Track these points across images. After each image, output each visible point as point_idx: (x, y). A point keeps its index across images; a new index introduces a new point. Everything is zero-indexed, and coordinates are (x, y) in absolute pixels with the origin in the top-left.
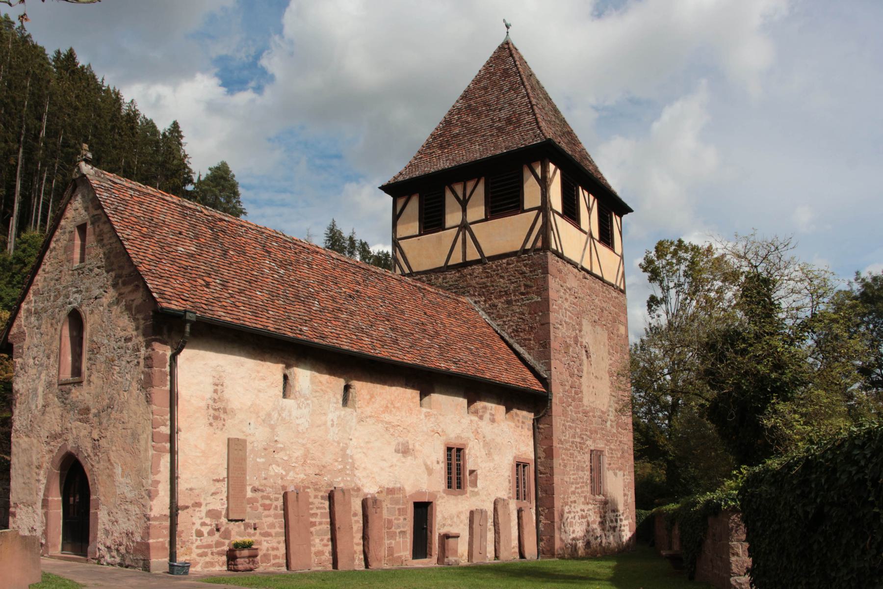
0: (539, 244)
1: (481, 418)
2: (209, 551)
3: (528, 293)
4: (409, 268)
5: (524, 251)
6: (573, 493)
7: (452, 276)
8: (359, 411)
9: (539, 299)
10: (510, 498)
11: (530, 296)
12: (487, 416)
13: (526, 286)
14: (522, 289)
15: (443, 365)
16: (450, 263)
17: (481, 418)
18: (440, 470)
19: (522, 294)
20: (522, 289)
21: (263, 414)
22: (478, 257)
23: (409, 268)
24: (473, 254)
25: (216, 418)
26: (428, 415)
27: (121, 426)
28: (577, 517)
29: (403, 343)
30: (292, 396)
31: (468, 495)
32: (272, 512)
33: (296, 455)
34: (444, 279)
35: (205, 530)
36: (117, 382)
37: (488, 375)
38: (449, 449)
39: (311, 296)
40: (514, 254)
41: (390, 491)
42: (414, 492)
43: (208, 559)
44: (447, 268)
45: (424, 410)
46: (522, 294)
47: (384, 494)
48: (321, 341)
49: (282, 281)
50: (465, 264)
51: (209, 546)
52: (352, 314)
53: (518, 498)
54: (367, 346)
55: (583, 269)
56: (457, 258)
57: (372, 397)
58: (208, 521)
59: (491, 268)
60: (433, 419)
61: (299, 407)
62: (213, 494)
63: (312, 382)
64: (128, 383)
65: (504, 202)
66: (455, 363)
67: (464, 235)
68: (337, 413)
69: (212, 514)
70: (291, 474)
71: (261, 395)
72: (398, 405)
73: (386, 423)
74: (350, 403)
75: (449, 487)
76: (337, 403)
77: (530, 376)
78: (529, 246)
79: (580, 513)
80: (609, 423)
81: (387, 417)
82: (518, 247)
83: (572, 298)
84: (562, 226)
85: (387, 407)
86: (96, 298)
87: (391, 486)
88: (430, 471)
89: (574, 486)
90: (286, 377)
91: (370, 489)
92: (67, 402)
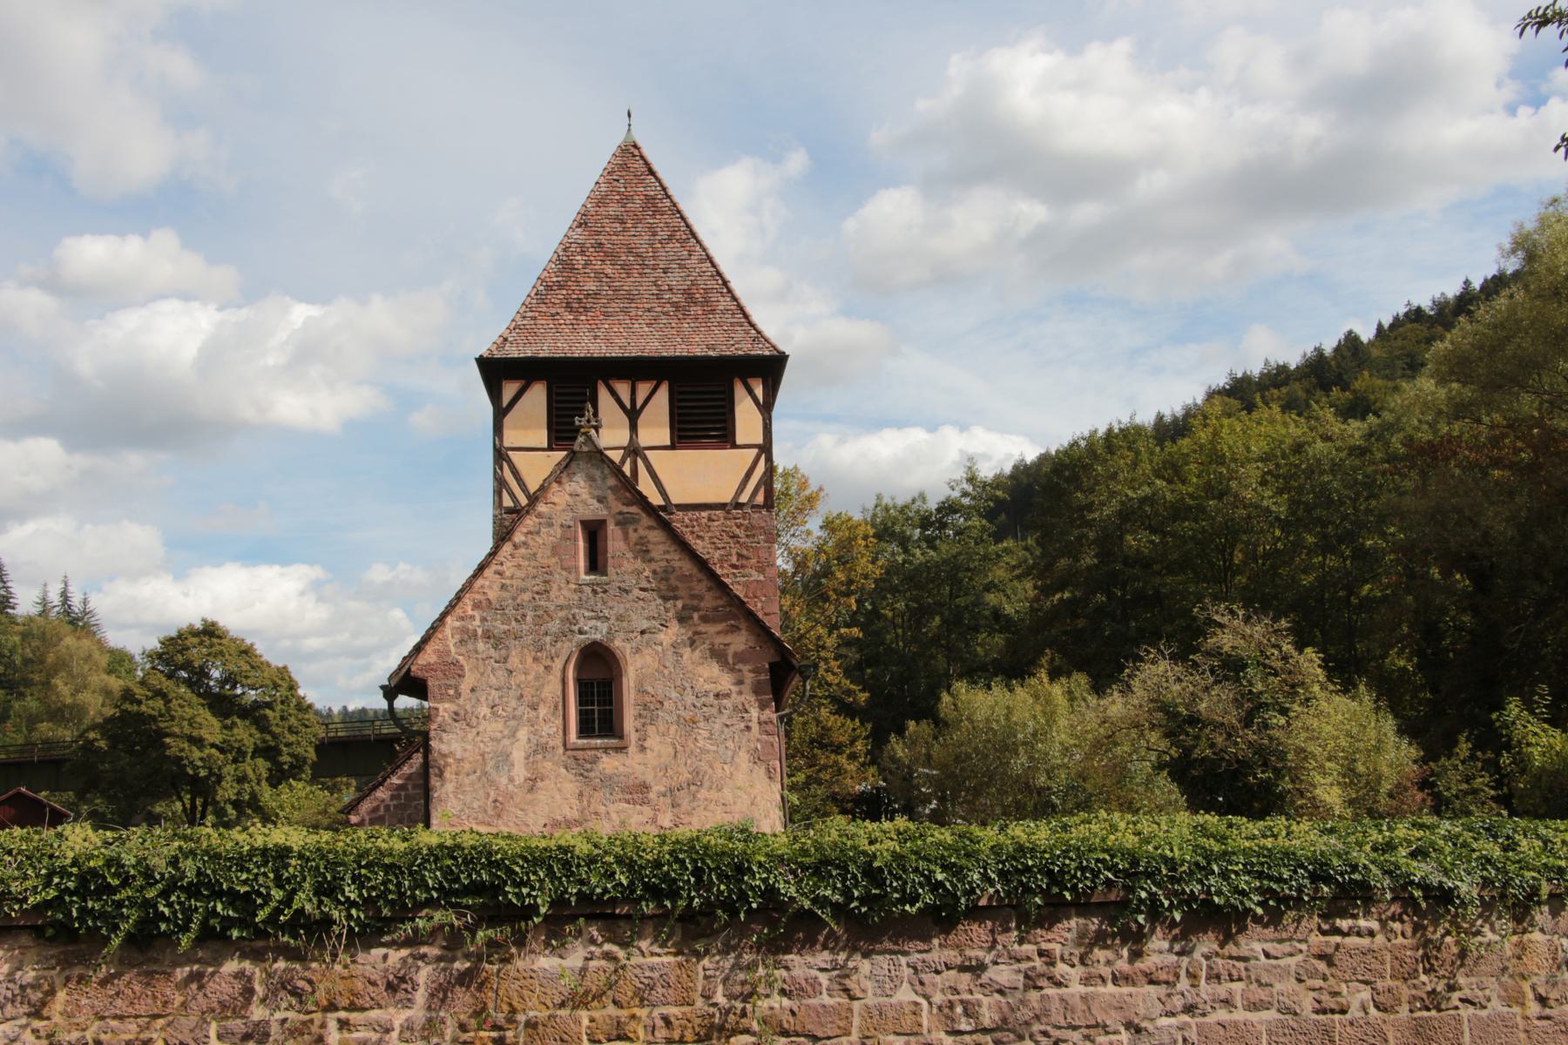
0: (760, 499)
3: (743, 567)
11: (746, 571)
13: (740, 556)
14: (734, 560)
19: (734, 566)
20: (734, 560)
27: (719, 809)
36: (704, 751)
40: (722, 506)
46: (734, 566)
64: (730, 753)
78: (744, 499)
82: (727, 498)
86: (643, 632)
92: (592, 774)
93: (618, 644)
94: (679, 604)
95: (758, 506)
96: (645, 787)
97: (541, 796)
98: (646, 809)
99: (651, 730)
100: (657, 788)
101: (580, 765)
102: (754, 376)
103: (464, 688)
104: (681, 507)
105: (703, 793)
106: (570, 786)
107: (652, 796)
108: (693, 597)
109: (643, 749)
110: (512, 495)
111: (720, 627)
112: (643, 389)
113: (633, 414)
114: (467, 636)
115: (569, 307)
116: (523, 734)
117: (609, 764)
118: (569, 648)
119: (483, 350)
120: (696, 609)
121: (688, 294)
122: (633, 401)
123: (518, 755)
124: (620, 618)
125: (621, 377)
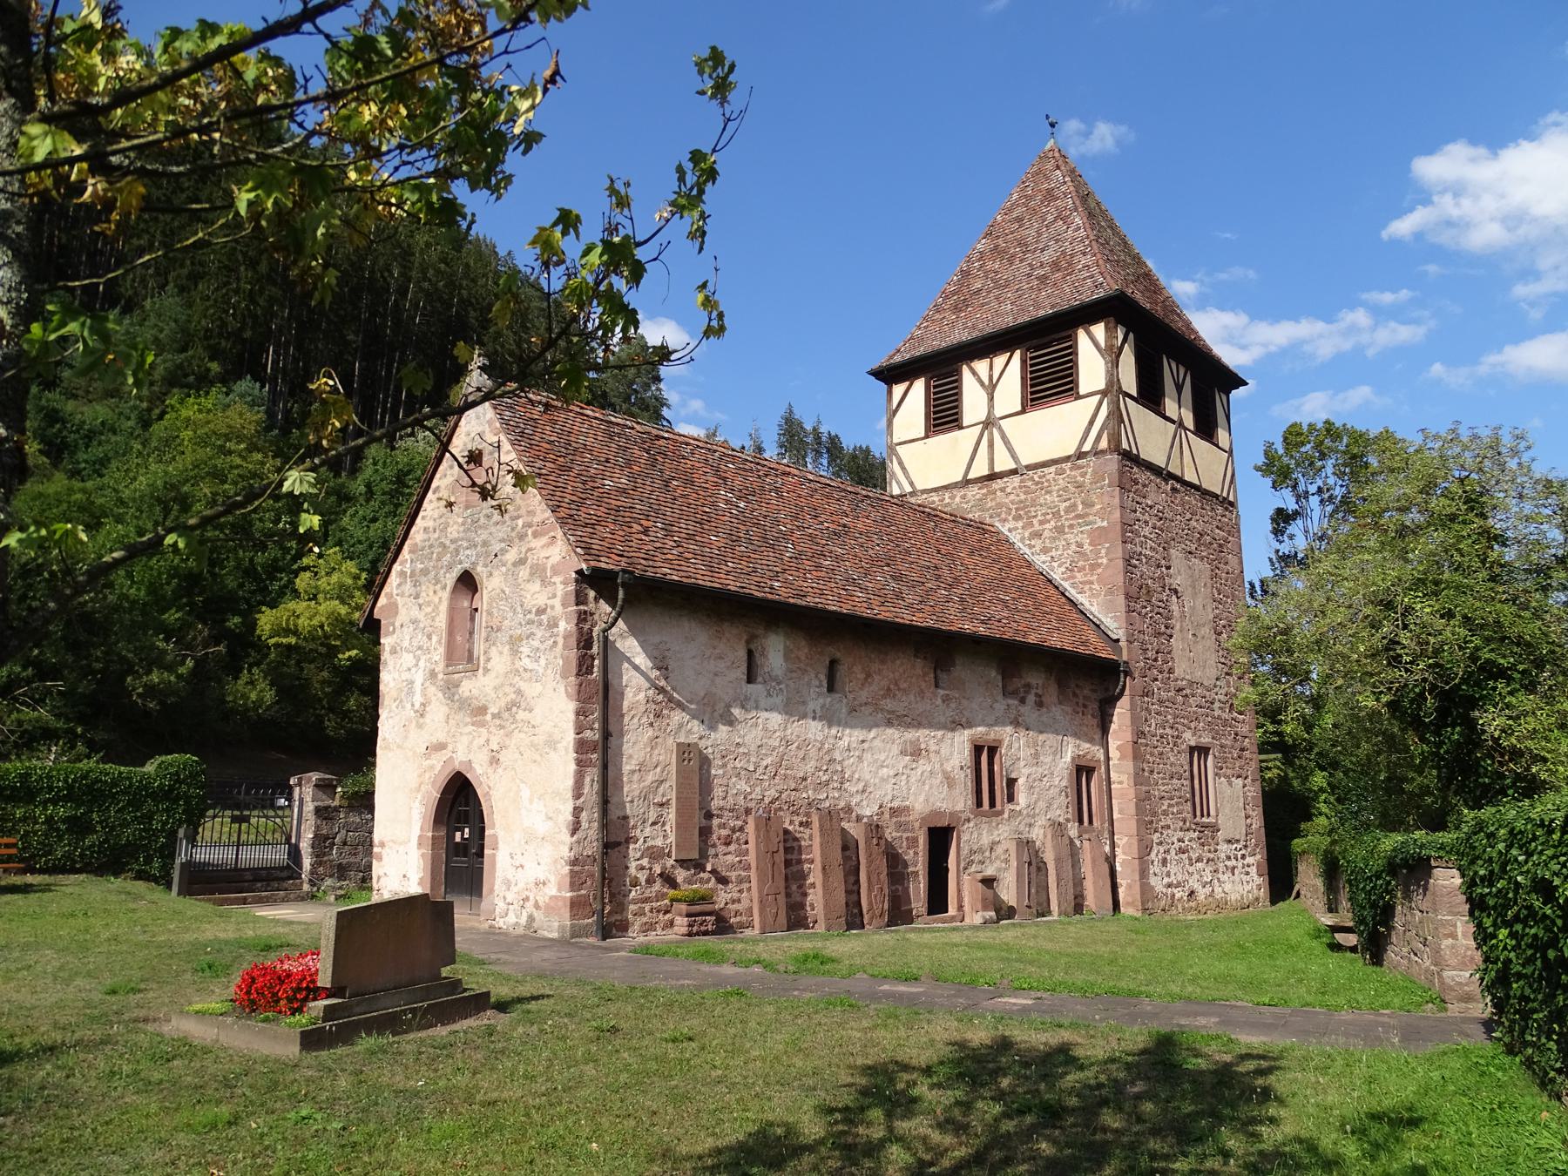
0: (1104, 444)
1: (1023, 701)
2: (647, 908)
3: (1087, 515)
4: (912, 484)
5: (1080, 455)
6: (1165, 813)
7: (974, 492)
8: (851, 696)
9: (1105, 524)
10: (1068, 820)
12: (1031, 698)
15: (968, 627)
16: (971, 476)
17: (1023, 701)
18: (965, 780)
19: (1078, 517)
21: (720, 707)
22: (1013, 466)
23: (912, 484)
24: (1003, 463)
25: (657, 716)
26: (946, 699)
28: (1173, 852)
29: (910, 598)
30: (760, 679)
31: (1006, 815)
32: (732, 848)
33: (764, 763)
34: (963, 497)
35: (642, 876)
37: (1032, 639)
38: (978, 750)
39: (786, 536)
40: (1068, 458)
41: (894, 812)
42: (927, 811)
43: (645, 920)
44: (966, 482)
45: (941, 692)
46: (1078, 517)
47: (887, 816)
48: (799, 602)
49: (742, 517)
50: (992, 477)
51: (646, 900)
52: (838, 558)
53: (1081, 821)
54: (861, 604)
55: (1171, 476)
56: (980, 469)
57: (868, 675)
58: (645, 862)
59: (1032, 479)
60: (953, 705)
61: (769, 695)
62: (654, 824)
63: (787, 657)
65: (1050, 382)
66: (983, 622)
67: (991, 434)
68: (821, 701)
69: (655, 854)
70: (758, 789)
71: (718, 680)
72: (904, 686)
73: (889, 712)
74: (838, 685)
75: (979, 804)
76: (820, 686)
77: (1093, 637)
78: (1087, 447)
79: (1177, 845)
80: (1217, 704)
81: (889, 704)
82: (1071, 451)
83: (1154, 520)
84: (1139, 415)
85: (889, 689)
87: (895, 804)
88: (949, 780)
89: (1166, 803)
90: (750, 653)
91: (868, 811)
93: (480, 572)
94: (520, 522)
95: (1102, 452)
96: (482, 710)
97: (428, 719)
98: (483, 730)
99: (493, 652)
100: (493, 709)
101: (450, 689)
102: (1095, 321)
103: (397, 624)
104: (1029, 468)
105: (521, 715)
106: (445, 709)
107: (489, 717)
108: (529, 513)
109: (486, 670)
110: (898, 483)
111: (544, 540)
112: (999, 361)
113: (991, 388)
114: (402, 574)
115: (956, 309)
116: (422, 664)
117: (468, 687)
118: (451, 579)
119: (875, 365)
120: (530, 525)
121: (1055, 266)
122: (991, 377)
123: (419, 677)
124: (485, 544)
125: (981, 356)
